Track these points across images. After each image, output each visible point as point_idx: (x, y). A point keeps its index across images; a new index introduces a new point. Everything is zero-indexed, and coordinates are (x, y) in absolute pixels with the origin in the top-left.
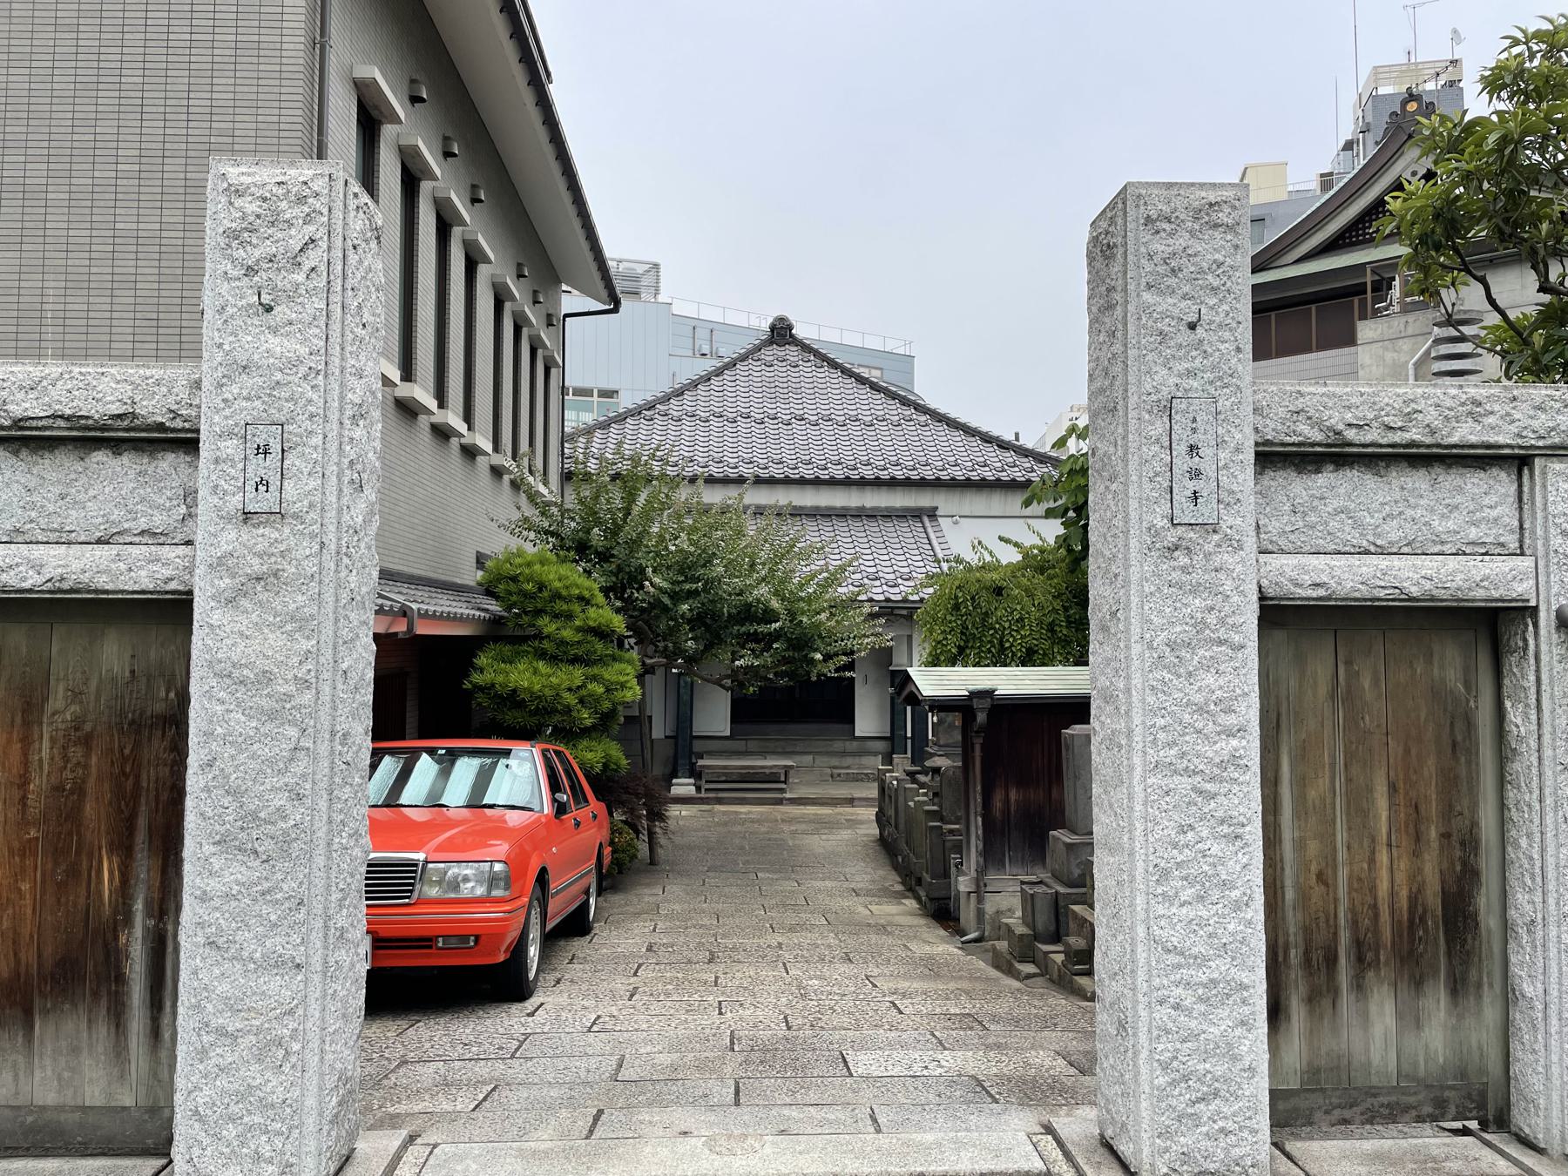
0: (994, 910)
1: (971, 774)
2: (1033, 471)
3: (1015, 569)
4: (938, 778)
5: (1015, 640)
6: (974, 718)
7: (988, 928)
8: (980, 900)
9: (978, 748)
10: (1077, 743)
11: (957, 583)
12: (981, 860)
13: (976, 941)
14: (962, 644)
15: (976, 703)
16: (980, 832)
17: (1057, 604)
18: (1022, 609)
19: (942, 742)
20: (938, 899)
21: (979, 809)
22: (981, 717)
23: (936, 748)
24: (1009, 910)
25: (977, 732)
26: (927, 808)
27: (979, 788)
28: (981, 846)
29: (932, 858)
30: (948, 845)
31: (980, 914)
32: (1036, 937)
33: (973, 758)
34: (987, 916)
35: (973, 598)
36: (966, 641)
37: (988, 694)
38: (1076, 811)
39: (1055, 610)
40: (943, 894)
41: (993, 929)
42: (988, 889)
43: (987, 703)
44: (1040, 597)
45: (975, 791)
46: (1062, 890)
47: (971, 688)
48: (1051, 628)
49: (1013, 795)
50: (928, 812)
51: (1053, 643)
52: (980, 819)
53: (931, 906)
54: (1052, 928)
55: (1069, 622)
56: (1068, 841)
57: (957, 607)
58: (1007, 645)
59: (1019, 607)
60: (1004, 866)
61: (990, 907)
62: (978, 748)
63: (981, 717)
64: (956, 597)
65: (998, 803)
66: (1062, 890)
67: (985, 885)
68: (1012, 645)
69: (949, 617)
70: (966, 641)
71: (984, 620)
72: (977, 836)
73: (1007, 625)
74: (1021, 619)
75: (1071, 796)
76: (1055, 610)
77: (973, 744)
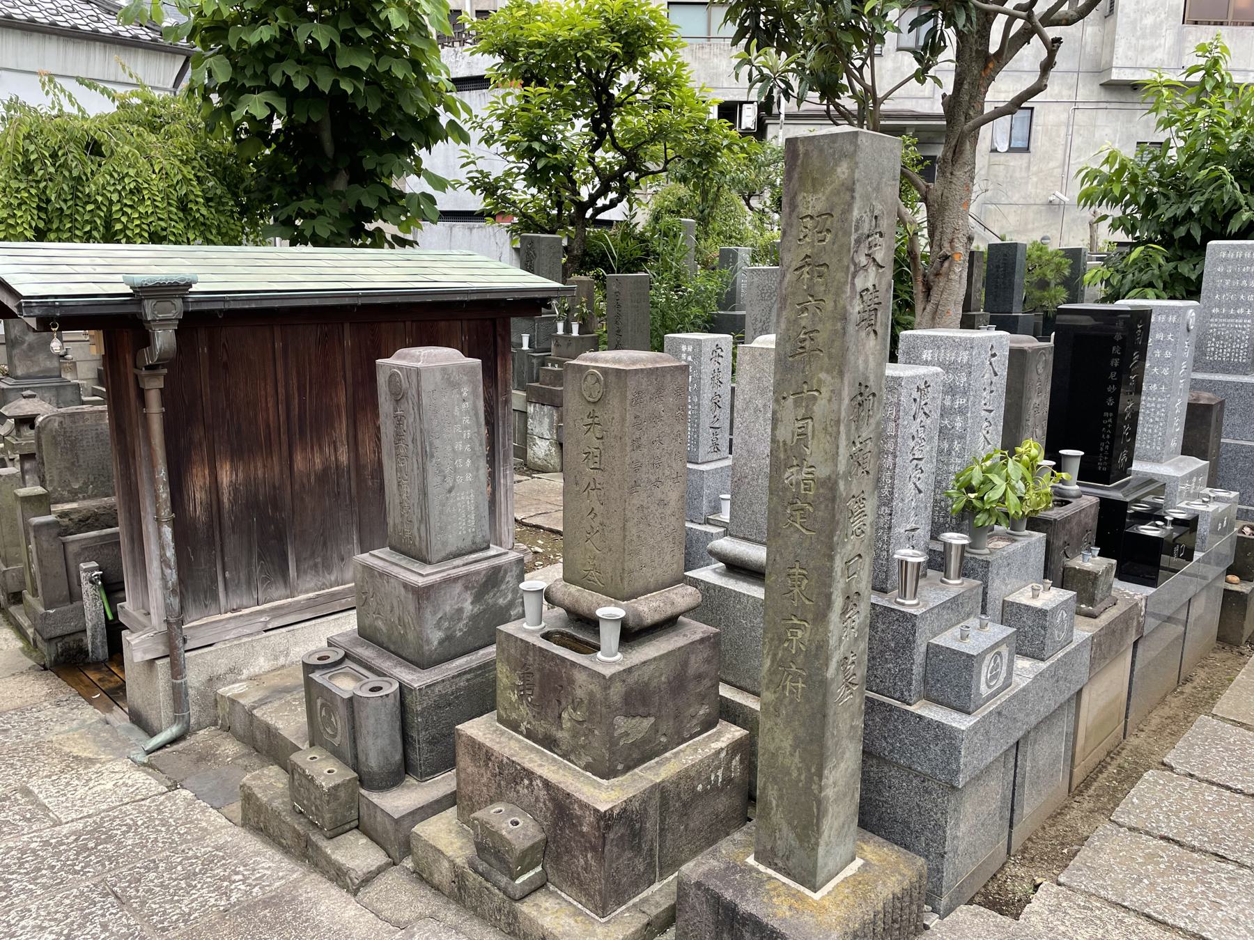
0: (204, 677)
1: (141, 450)
2: (99, 20)
3: (113, 123)
4: (28, 432)
5: (131, 220)
6: (145, 339)
7: (194, 710)
8: (177, 670)
9: (154, 399)
10: (427, 386)
11: (24, 130)
12: (175, 602)
13: (173, 741)
14: (41, 225)
15: (150, 310)
16: (170, 553)
17: (188, 172)
18: (138, 174)
19: (19, 372)
20: (62, 637)
21: (166, 512)
22: (164, 339)
23: (11, 381)
24: (231, 671)
25: (149, 368)
26: (22, 492)
27: (162, 474)
28: (172, 576)
29: (44, 575)
30: (72, 549)
31: (179, 696)
32: (365, 780)
33: (146, 417)
34: (191, 692)
35: (54, 156)
36: (49, 221)
37: (176, 290)
38: (425, 519)
39: (186, 180)
40: (72, 626)
41: (203, 709)
42: (188, 647)
43: (175, 310)
44: (161, 162)
45: (153, 481)
46: (416, 679)
47: (139, 279)
48: (183, 205)
49: (226, 476)
50: (26, 499)
51: (187, 227)
52: (167, 531)
53: (49, 652)
54: (398, 757)
55: (208, 200)
56: (421, 582)
57: (28, 168)
58: (118, 227)
59: (132, 172)
60: (215, 598)
61: (194, 678)
62: (154, 399)
63: (164, 339)
64: (26, 153)
65: (198, 492)
66: (416, 679)
67: (185, 641)
68: (126, 227)
69: (14, 184)
70: (49, 221)
71: (74, 189)
72: (164, 561)
73: (115, 197)
74: (138, 190)
75: (411, 491)
76: (186, 180)
77: (142, 395)
